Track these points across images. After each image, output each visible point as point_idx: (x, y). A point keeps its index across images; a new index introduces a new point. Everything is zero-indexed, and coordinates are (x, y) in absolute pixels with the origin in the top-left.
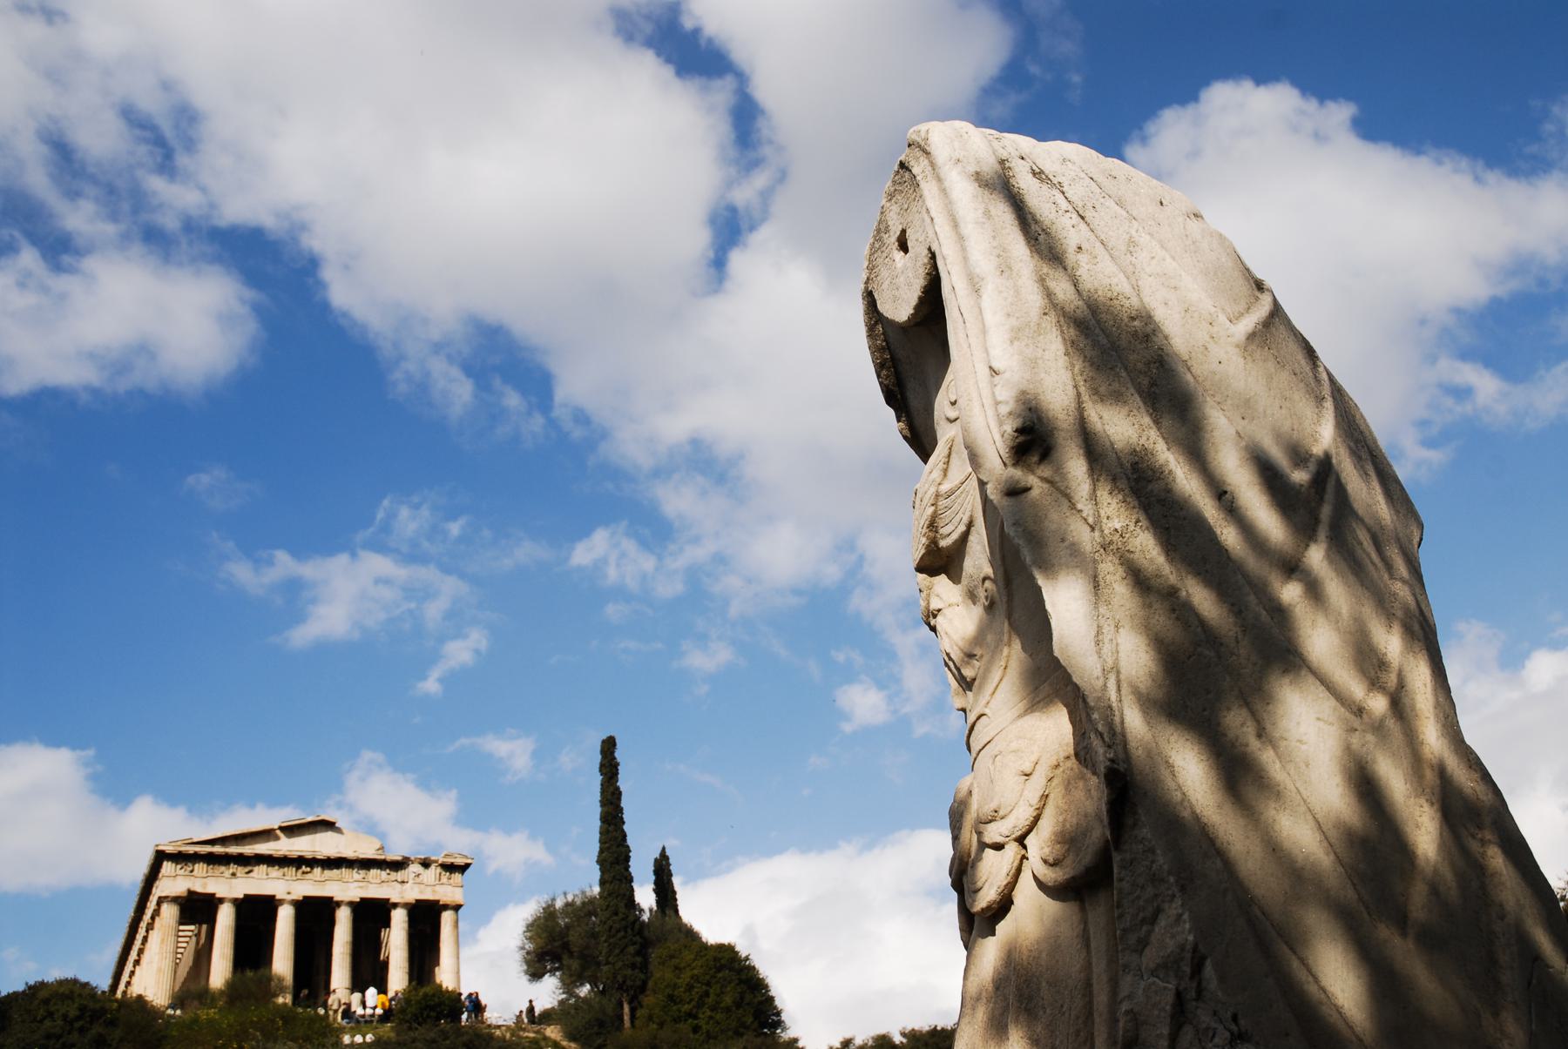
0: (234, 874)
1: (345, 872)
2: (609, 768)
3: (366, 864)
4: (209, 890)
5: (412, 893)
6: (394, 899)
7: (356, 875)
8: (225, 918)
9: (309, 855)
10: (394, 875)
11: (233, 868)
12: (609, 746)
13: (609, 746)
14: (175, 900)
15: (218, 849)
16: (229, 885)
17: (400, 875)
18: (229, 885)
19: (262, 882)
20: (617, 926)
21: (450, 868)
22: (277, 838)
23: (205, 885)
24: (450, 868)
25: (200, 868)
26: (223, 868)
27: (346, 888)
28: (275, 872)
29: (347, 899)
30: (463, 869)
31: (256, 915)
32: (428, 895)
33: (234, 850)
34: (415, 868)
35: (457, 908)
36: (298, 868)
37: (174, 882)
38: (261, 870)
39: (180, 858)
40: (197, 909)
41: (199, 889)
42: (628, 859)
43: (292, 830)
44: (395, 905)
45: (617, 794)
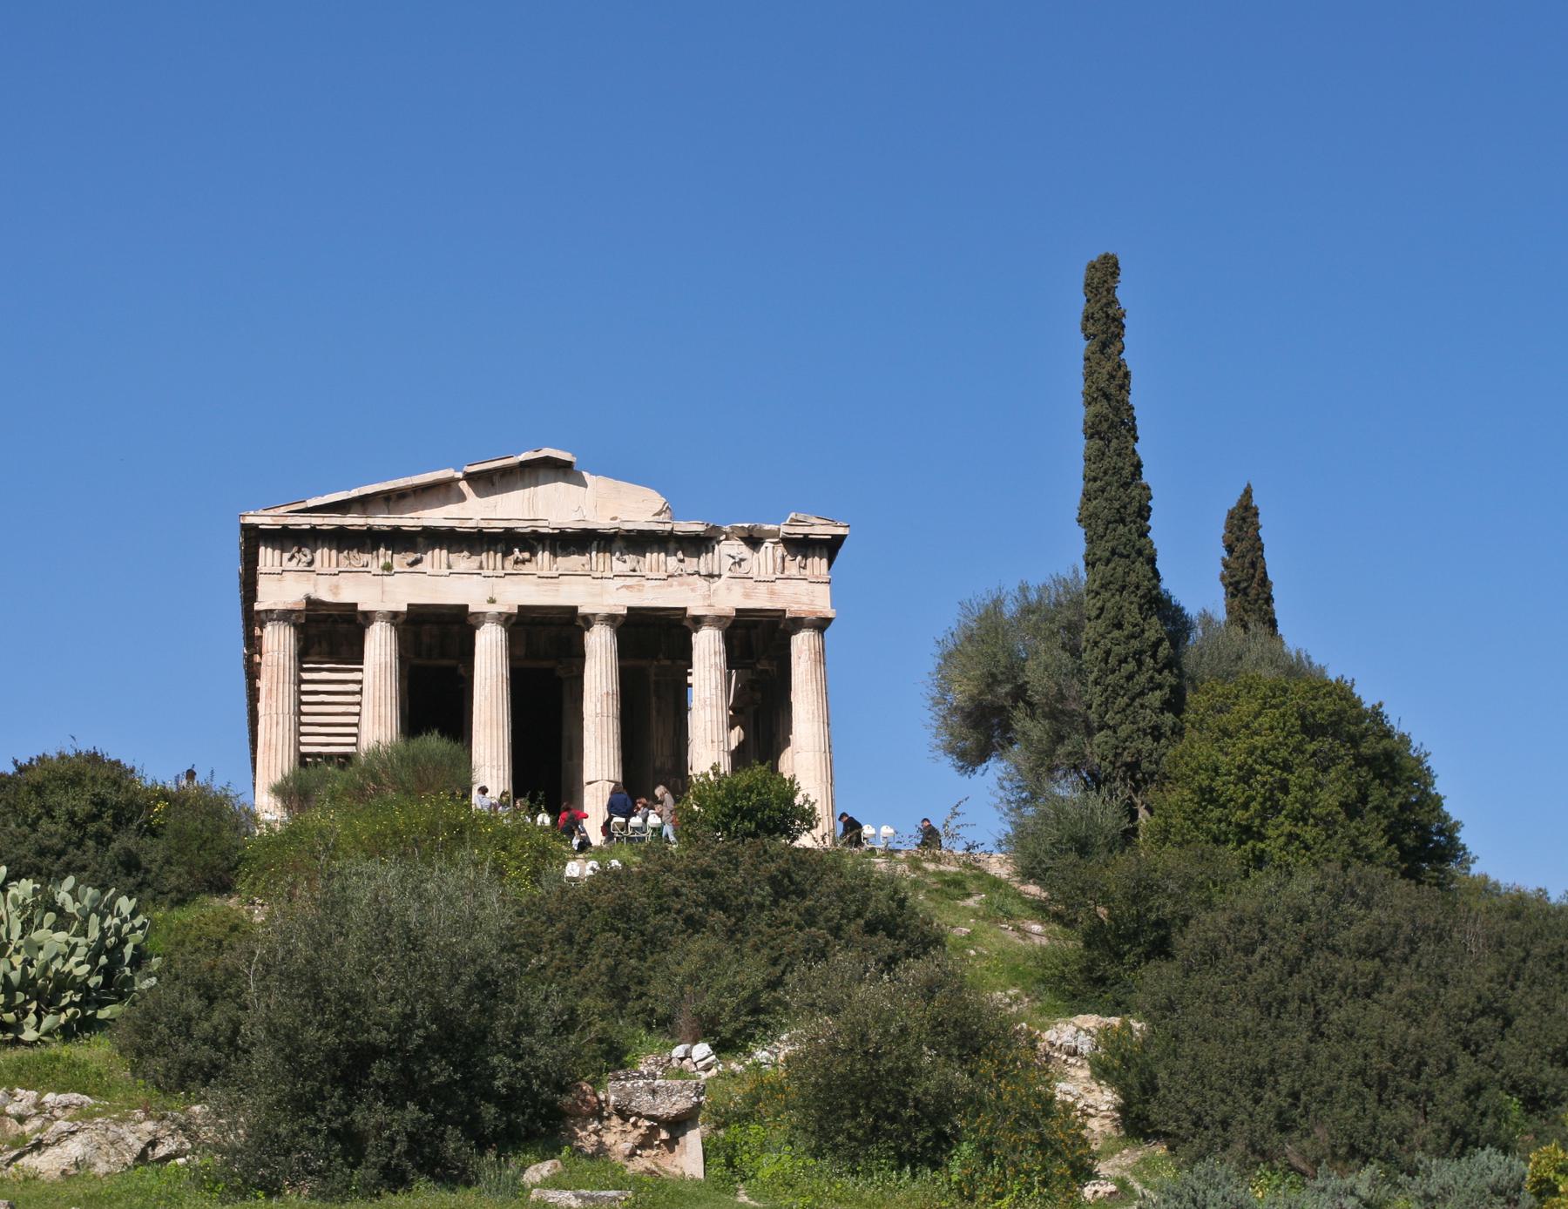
0: (388, 567)
1: (597, 560)
2: (1105, 327)
3: (639, 542)
4: (345, 597)
5: (729, 598)
6: (695, 610)
7: (620, 564)
8: (380, 645)
9: (523, 527)
10: (691, 564)
11: (384, 555)
12: (1103, 278)
13: (1103, 278)
14: (285, 616)
15: (353, 521)
16: (381, 588)
17: (705, 563)
18: (381, 588)
19: (442, 582)
20: (1119, 650)
21: (801, 546)
22: (462, 498)
23: (335, 589)
24: (801, 546)
25: (325, 557)
26: (366, 557)
27: (600, 590)
28: (463, 561)
29: (603, 610)
30: (830, 548)
31: (434, 641)
32: (760, 600)
33: (382, 521)
34: (736, 548)
35: (821, 625)
36: (506, 554)
37: (285, 584)
38: (436, 558)
39: (285, 538)
40: (330, 634)
41: (328, 597)
42: (1144, 512)
43: (487, 482)
44: (698, 621)
45: (1121, 377)
